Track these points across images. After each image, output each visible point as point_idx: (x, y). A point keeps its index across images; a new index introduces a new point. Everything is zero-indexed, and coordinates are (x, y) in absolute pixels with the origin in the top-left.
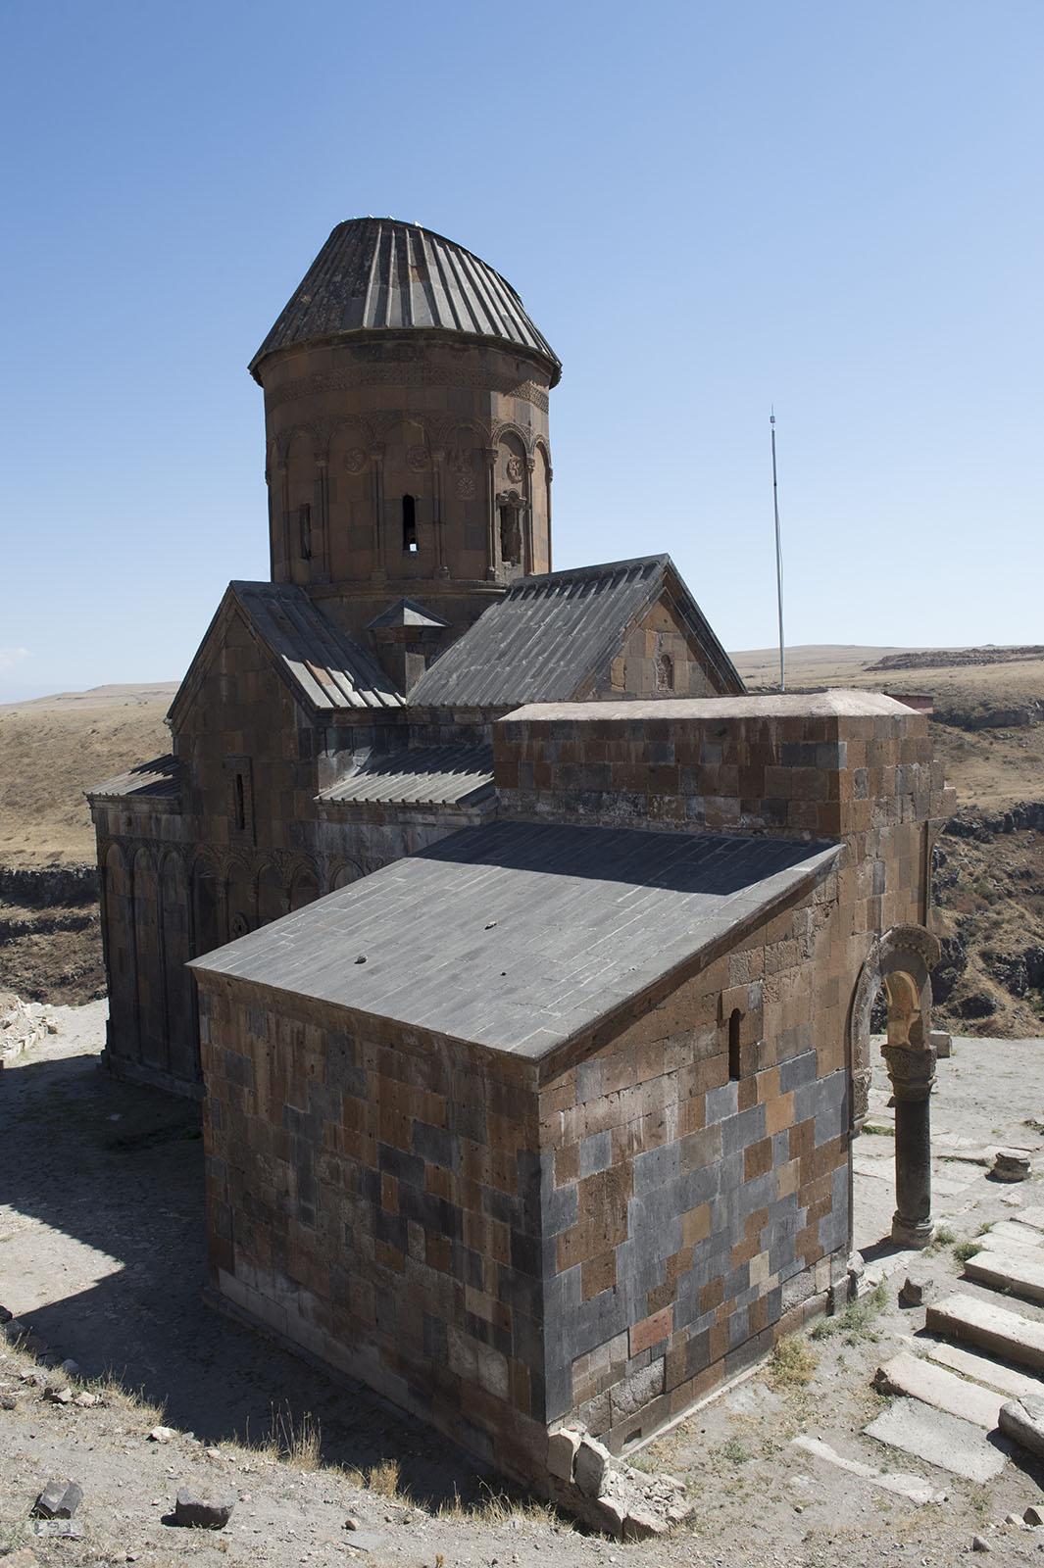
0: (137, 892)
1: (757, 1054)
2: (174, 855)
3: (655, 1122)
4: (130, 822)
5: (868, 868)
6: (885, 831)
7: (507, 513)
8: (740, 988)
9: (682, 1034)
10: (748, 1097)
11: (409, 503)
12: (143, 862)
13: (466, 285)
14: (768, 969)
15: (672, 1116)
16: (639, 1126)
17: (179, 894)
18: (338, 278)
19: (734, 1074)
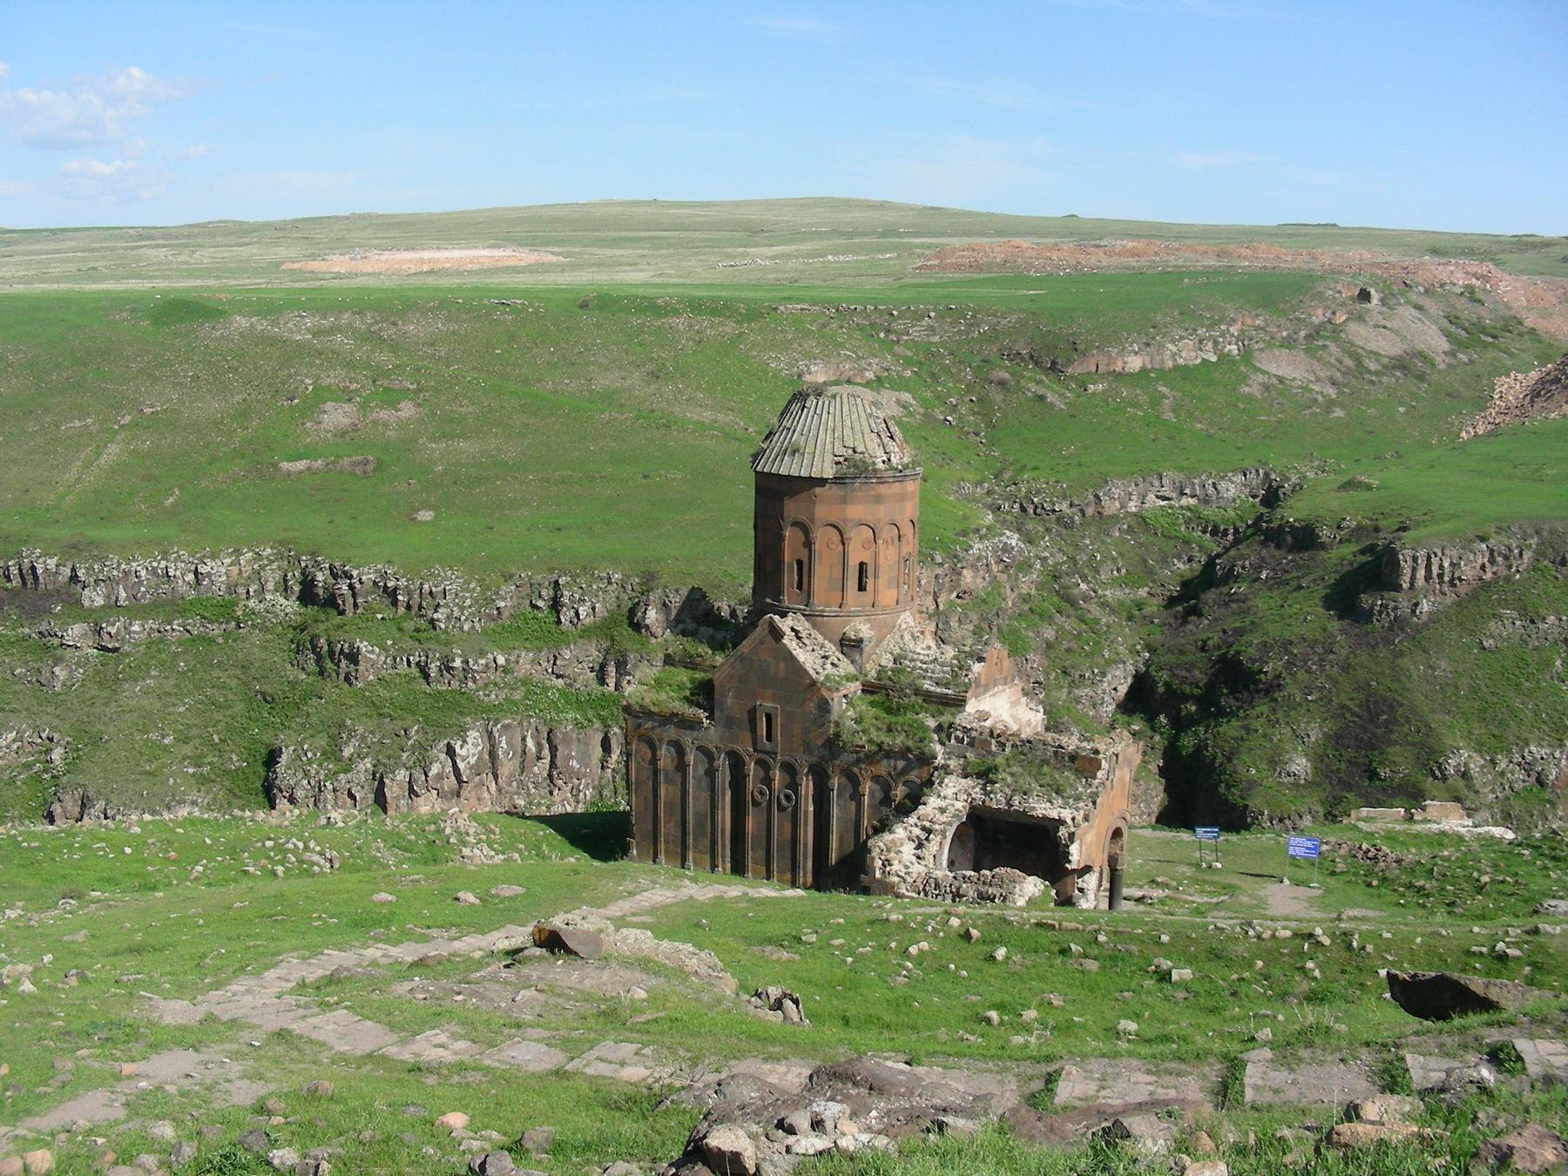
11: (862, 567)
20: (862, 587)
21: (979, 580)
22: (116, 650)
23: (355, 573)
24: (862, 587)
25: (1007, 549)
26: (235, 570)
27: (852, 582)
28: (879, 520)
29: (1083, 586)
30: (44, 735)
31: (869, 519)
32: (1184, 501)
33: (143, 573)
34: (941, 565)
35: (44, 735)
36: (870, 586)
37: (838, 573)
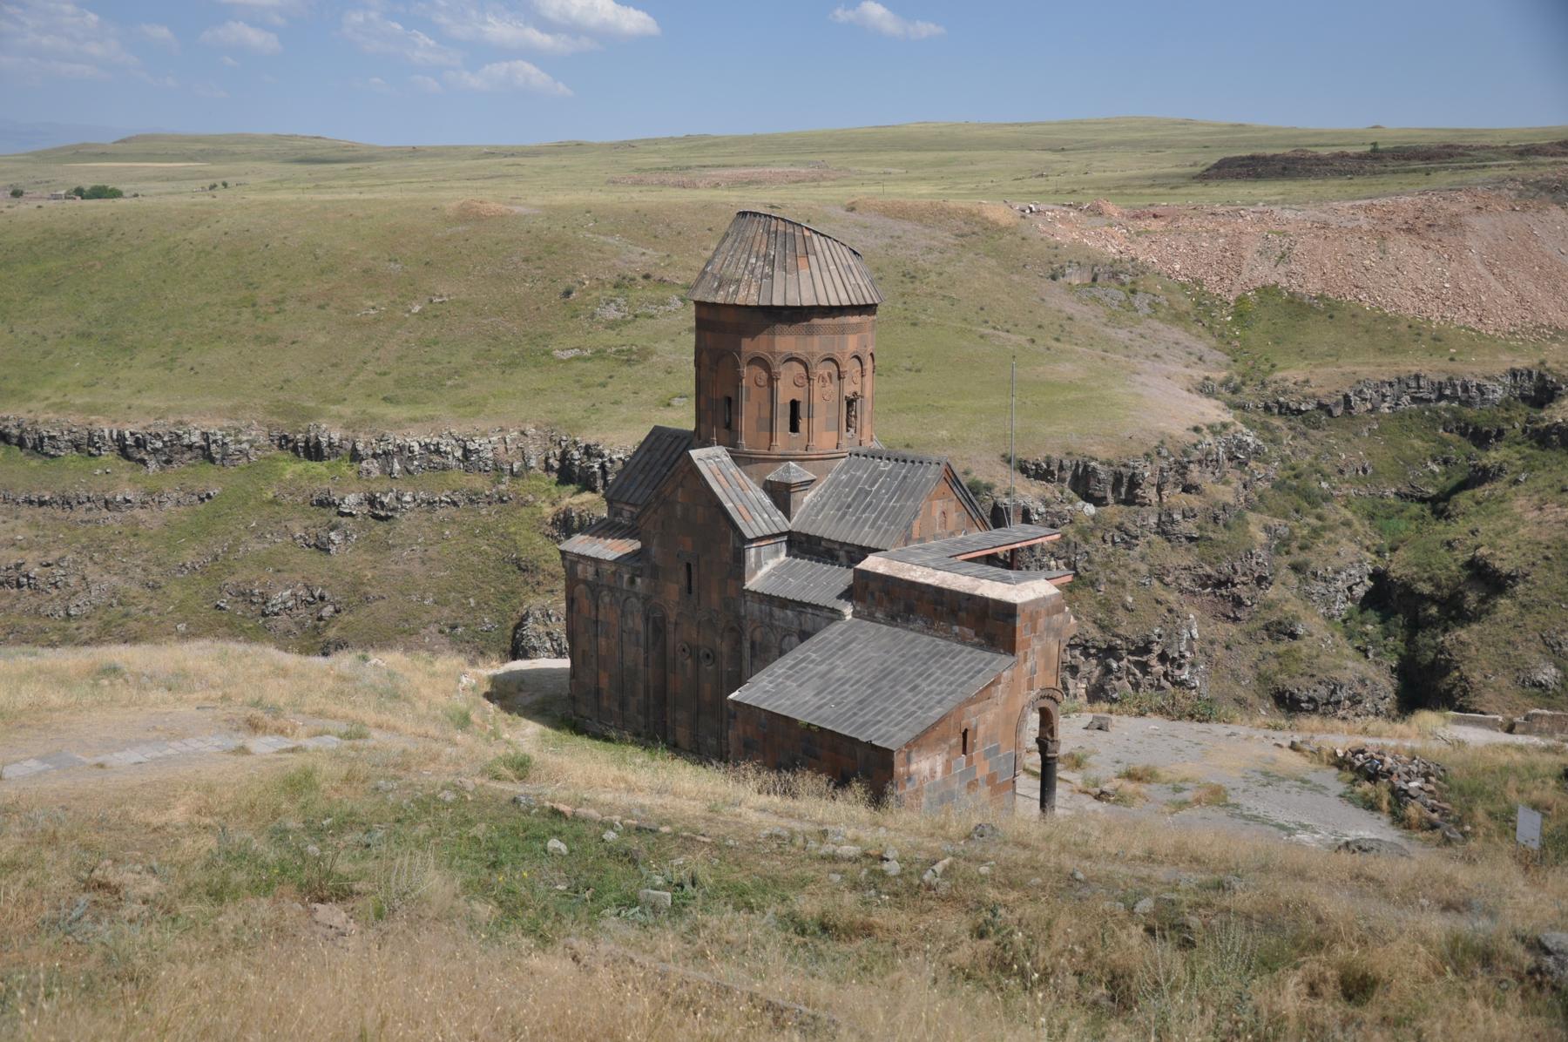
0: (601, 617)
1: (974, 745)
2: (633, 600)
3: (933, 772)
4: (597, 573)
5: (1029, 664)
6: (1038, 647)
7: (850, 403)
8: (970, 721)
9: (944, 739)
10: (970, 761)
11: (794, 405)
12: (607, 599)
13: (832, 267)
14: (980, 711)
15: (939, 769)
16: (927, 773)
17: (637, 623)
18: (753, 260)
19: (964, 752)
20: (794, 427)
21: (1208, 475)
22: (387, 518)
23: (606, 452)
24: (794, 427)
25: (1241, 446)
26: (501, 448)
27: (783, 421)
28: (813, 354)
29: (1324, 485)
30: (317, 594)
31: (800, 352)
32: (1443, 404)
33: (417, 448)
34: (1166, 458)
35: (317, 594)
36: (803, 425)
37: (766, 413)
